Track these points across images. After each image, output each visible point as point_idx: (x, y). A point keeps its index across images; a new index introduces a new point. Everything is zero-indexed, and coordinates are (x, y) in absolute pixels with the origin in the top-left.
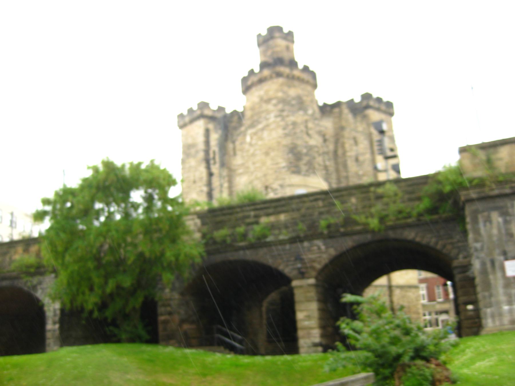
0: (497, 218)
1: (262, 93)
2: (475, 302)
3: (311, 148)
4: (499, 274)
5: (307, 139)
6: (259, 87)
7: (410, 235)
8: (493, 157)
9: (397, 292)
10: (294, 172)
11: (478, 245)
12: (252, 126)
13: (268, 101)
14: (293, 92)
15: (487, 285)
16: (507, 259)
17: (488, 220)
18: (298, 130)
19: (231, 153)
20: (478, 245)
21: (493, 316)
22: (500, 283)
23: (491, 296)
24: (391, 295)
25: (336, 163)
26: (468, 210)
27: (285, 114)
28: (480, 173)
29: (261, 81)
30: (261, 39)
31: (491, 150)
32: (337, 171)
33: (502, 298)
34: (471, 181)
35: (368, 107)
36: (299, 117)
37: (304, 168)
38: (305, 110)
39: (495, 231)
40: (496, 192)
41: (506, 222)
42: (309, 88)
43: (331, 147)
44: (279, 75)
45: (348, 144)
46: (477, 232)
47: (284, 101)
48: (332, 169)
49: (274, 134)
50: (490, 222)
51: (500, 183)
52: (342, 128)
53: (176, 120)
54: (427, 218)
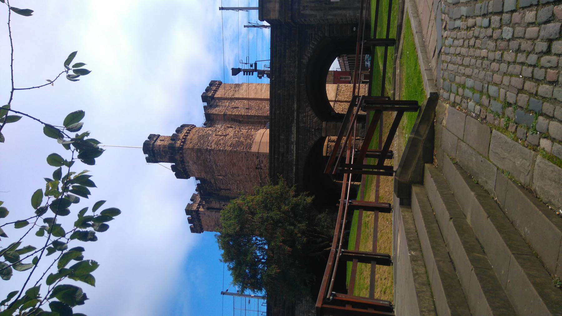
1: (191, 162)
3: (235, 136)
5: (228, 137)
7: (305, 61)
9: (340, 98)
19: (228, 192)
29: (183, 162)
45: (235, 112)
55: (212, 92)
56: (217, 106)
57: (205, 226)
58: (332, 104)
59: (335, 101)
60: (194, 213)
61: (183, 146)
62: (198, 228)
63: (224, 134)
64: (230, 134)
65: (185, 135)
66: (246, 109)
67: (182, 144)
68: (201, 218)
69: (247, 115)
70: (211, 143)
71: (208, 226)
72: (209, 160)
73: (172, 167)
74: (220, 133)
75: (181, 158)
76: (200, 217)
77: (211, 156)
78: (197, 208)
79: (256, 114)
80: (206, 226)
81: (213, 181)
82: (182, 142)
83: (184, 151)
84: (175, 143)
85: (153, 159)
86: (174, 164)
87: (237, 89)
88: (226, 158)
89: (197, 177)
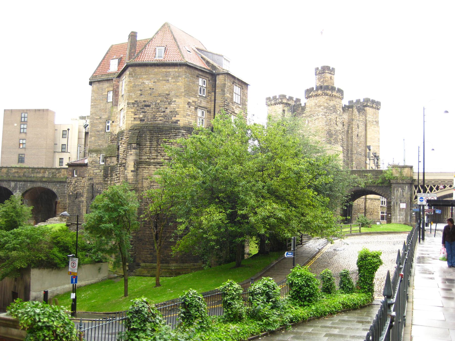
0: (400, 190)
2: (391, 214)
3: (336, 131)
4: (398, 207)
5: (336, 127)
6: (315, 98)
8: (402, 171)
10: (328, 143)
11: (393, 197)
12: (310, 116)
13: (320, 106)
14: (332, 103)
15: (394, 210)
16: (401, 203)
17: (398, 190)
18: (332, 123)
20: (393, 197)
21: (394, 219)
22: (398, 209)
23: (395, 213)
24: (365, 203)
25: (348, 137)
26: (393, 186)
27: (327, 114)
28: (397, 175)
29: (316, 95)
30: (318, 71)
31: (403, 169)
32: (347, 141)
33: (398, 214)
34: (394, 178)
35: (366, 106)
36: (333, 116)
37: (333, 141)
38: (336, 112)
39: (399, 194)
40: (401, 182)
41: (402, 191)
42: (339, 100)
43: (346, 129)
44: (327, 95)
45: (355, 127)
46: (394, 193)
47: (326, 108)
48: (345, 140)
49: (321, 124)
50: (398, 191)
51: (403, 180)
52: (353, 120)
53: (265, 101)
54: (380, 185)
55: (371, 105)
56: (359, 112)
57: (270, 108)
58: (364, 197)
59: (366, 199)
60: (280, 100)
61: (328, 95)
62: (269, 103)
63: (337, 123)
64: (338, 127)
65: (335, 96)
66: (358, 135)
67: (329, 95)
68: (277, 105)
69: (352, 136)
70: (331, 115)
71: (271, 110)
72: (318, 114)
73: (313, 88)
74: (338, 120)
75: (319, 94)
76: (278, 104)
77: (321, 116)
78: (284, 103)
79: (353, 143)
80: (271, 109)
81: (304, 115)
82: (330, 95)
83: (324, 96)
84: (330, 90)
85: (317, 73)
86: (315, 89)
87: (374, 123)
88: (321, 127)
89: (307, 104)
